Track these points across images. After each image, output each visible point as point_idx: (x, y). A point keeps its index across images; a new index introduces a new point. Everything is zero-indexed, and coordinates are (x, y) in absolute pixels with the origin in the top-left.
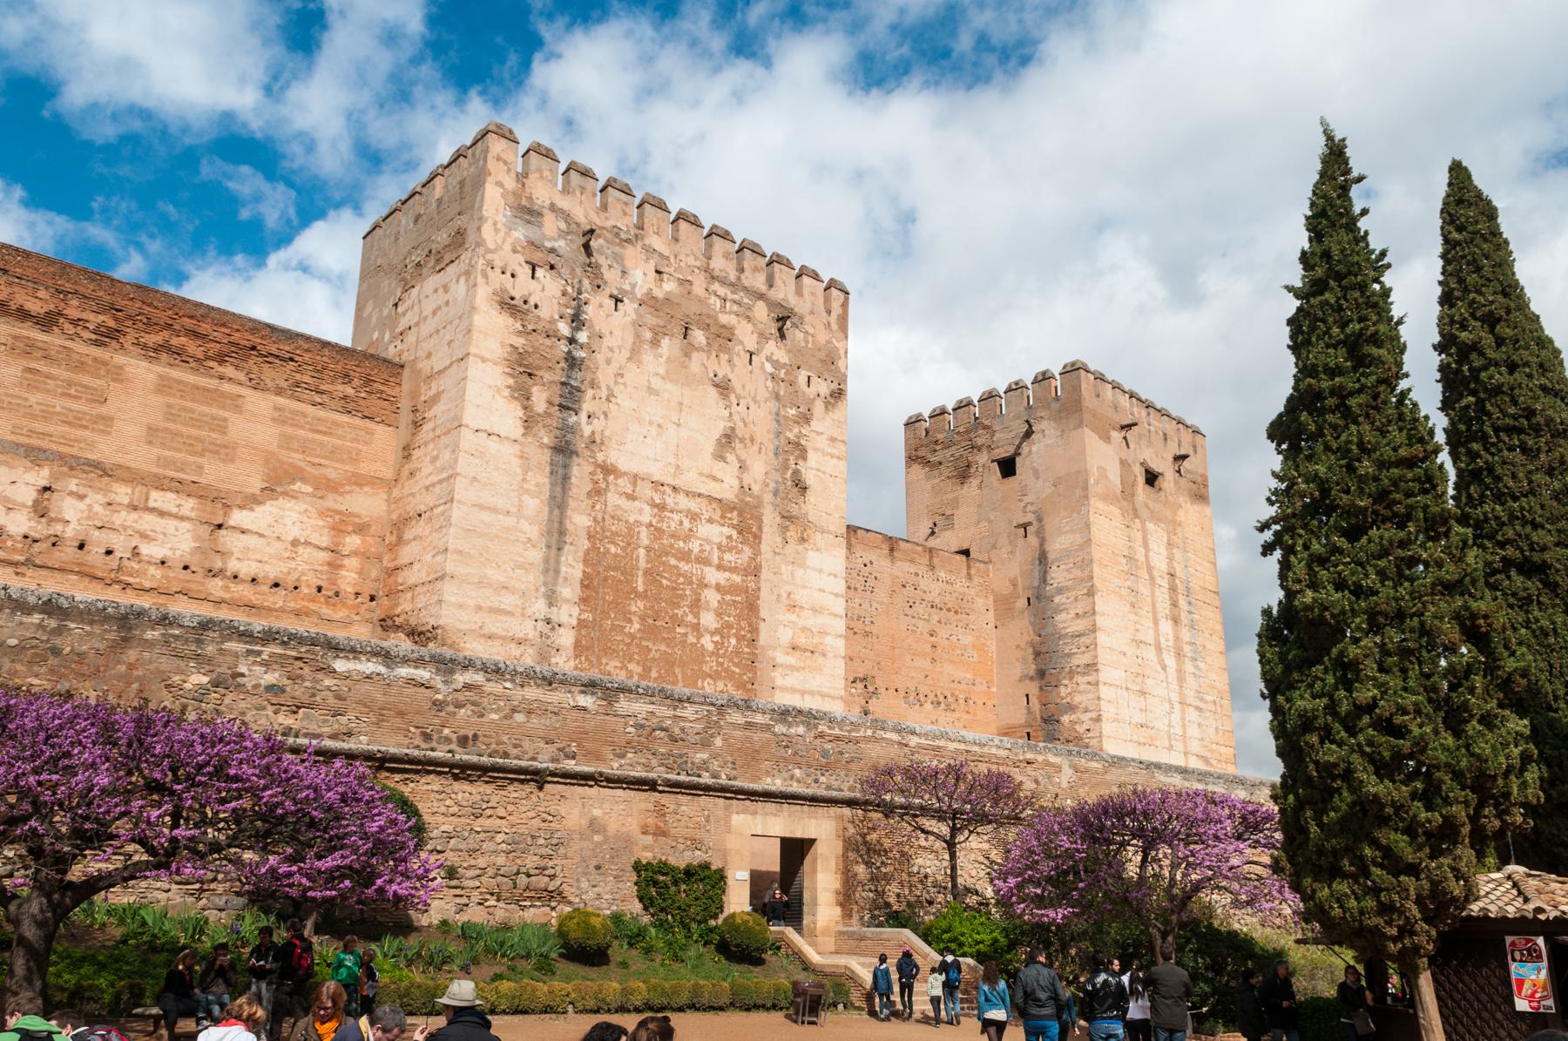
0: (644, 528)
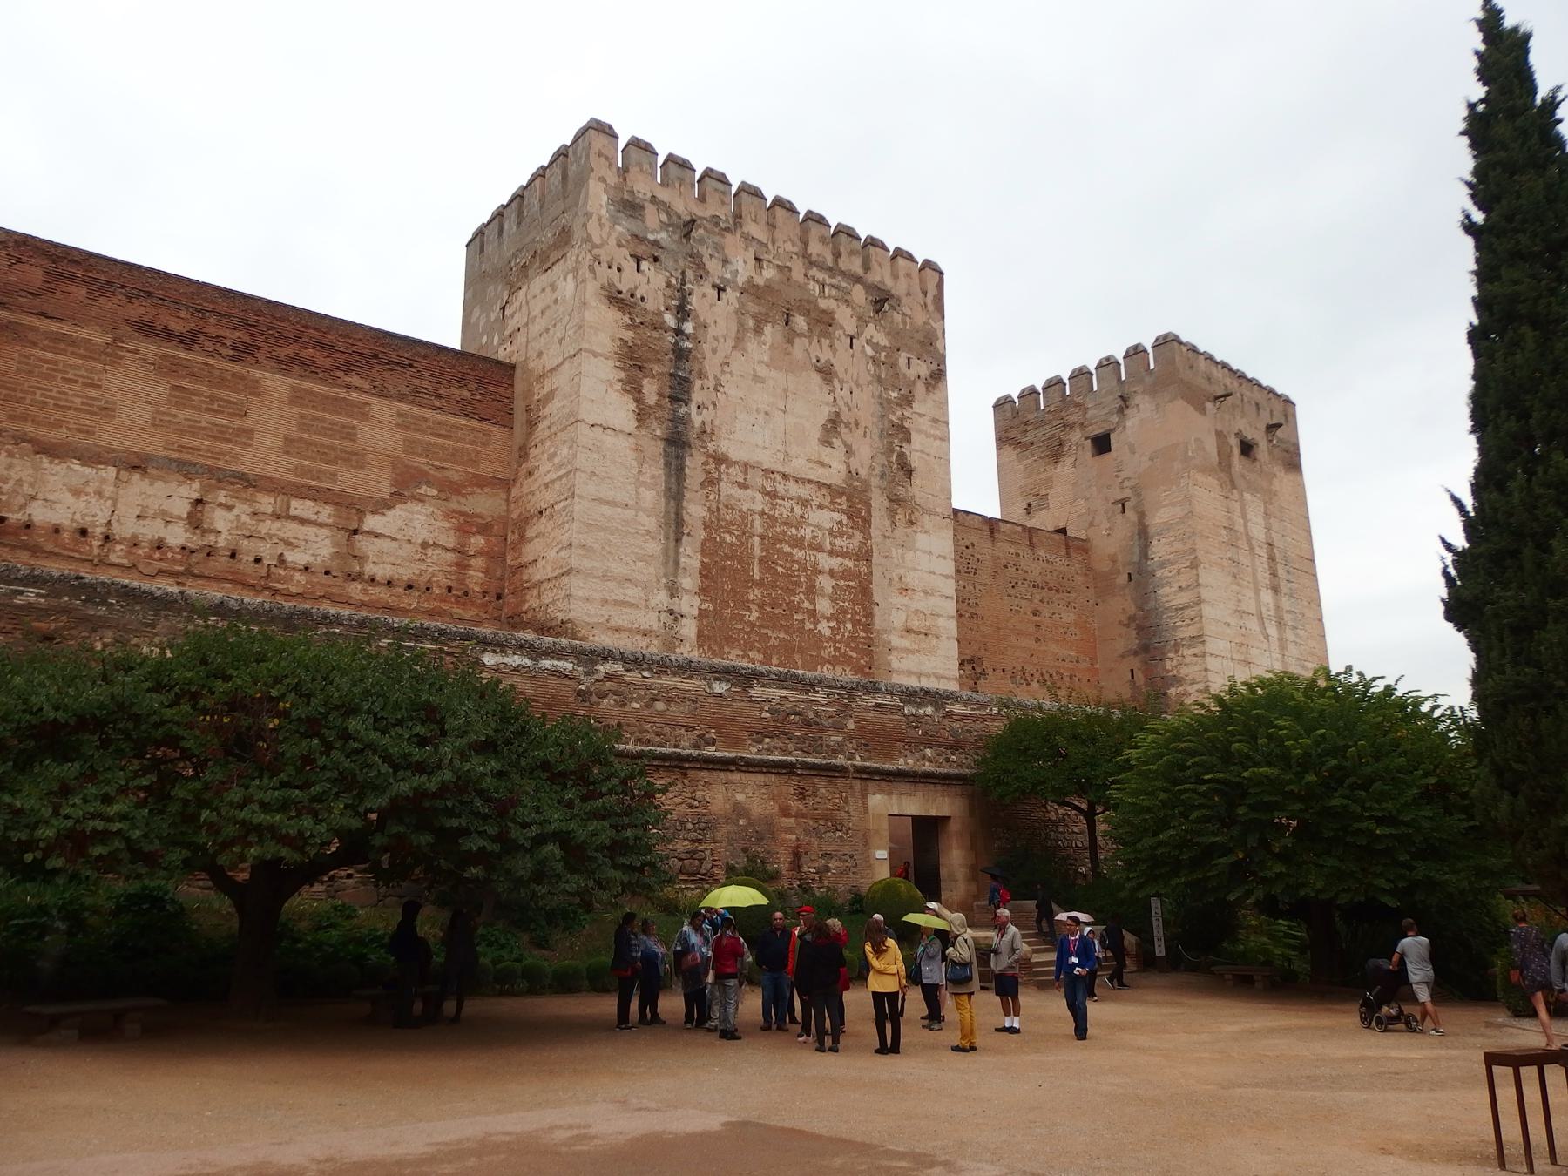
0: (757, 516)
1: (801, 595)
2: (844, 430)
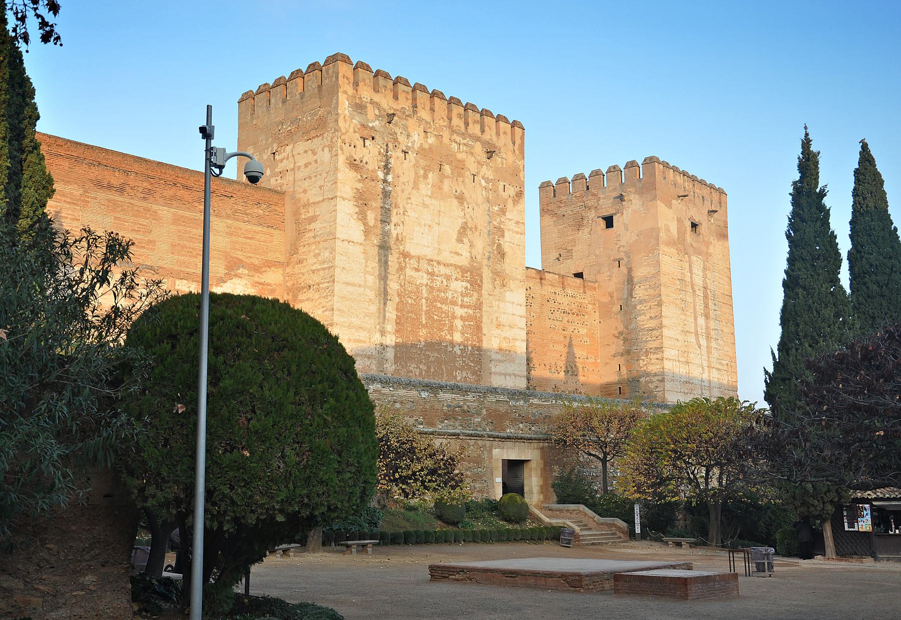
0: (424, 287)
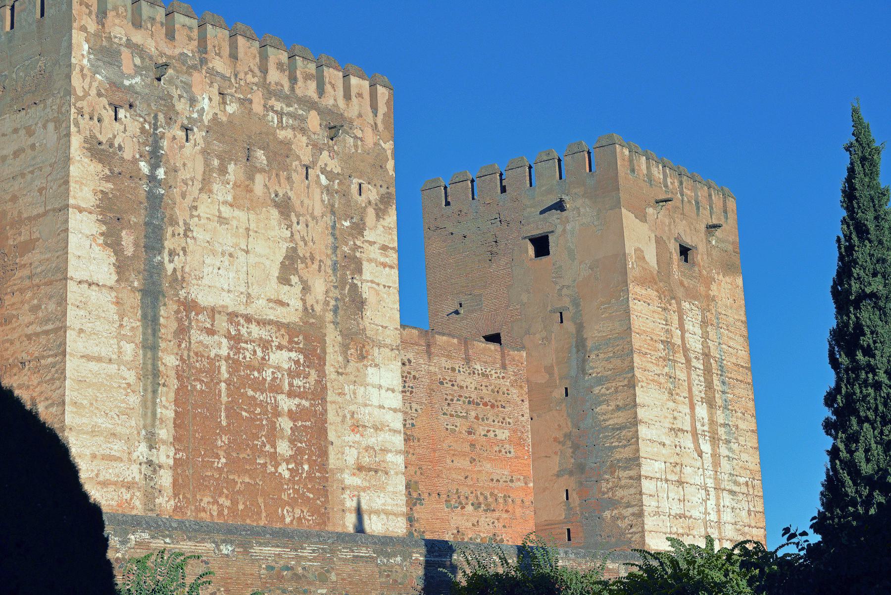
0: (224, 362)
1: (263, 438)
2: (301, 266)
